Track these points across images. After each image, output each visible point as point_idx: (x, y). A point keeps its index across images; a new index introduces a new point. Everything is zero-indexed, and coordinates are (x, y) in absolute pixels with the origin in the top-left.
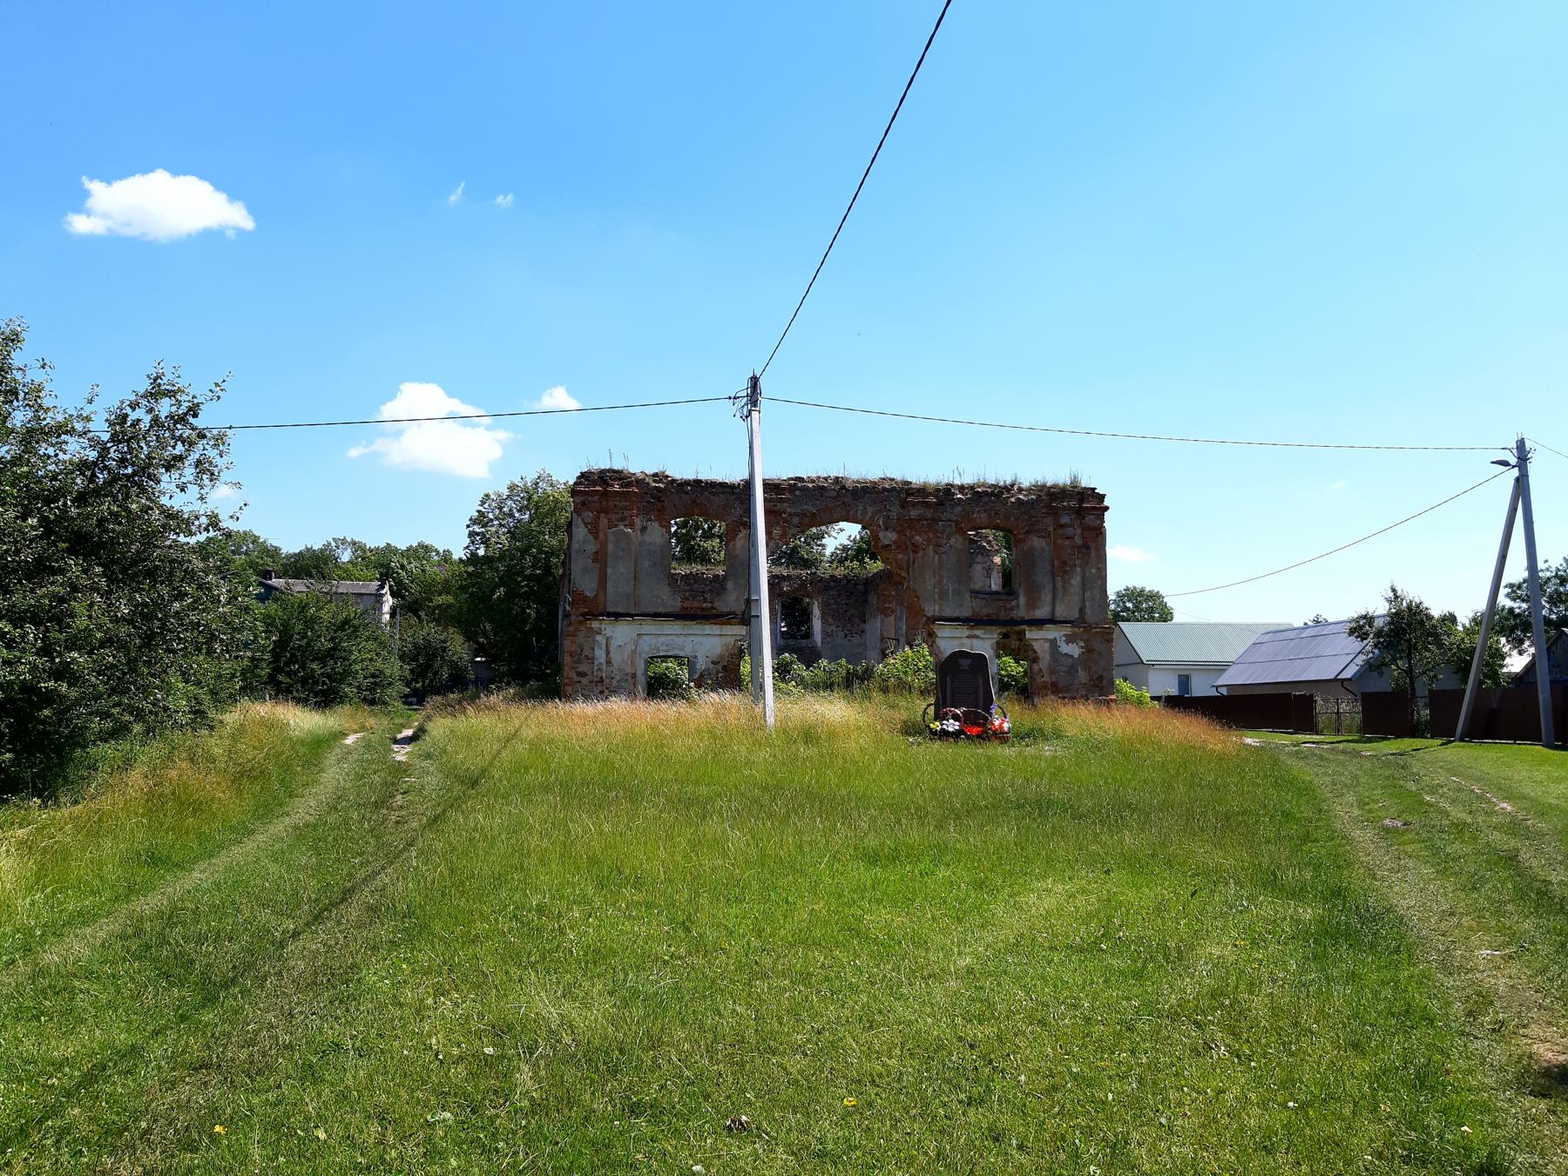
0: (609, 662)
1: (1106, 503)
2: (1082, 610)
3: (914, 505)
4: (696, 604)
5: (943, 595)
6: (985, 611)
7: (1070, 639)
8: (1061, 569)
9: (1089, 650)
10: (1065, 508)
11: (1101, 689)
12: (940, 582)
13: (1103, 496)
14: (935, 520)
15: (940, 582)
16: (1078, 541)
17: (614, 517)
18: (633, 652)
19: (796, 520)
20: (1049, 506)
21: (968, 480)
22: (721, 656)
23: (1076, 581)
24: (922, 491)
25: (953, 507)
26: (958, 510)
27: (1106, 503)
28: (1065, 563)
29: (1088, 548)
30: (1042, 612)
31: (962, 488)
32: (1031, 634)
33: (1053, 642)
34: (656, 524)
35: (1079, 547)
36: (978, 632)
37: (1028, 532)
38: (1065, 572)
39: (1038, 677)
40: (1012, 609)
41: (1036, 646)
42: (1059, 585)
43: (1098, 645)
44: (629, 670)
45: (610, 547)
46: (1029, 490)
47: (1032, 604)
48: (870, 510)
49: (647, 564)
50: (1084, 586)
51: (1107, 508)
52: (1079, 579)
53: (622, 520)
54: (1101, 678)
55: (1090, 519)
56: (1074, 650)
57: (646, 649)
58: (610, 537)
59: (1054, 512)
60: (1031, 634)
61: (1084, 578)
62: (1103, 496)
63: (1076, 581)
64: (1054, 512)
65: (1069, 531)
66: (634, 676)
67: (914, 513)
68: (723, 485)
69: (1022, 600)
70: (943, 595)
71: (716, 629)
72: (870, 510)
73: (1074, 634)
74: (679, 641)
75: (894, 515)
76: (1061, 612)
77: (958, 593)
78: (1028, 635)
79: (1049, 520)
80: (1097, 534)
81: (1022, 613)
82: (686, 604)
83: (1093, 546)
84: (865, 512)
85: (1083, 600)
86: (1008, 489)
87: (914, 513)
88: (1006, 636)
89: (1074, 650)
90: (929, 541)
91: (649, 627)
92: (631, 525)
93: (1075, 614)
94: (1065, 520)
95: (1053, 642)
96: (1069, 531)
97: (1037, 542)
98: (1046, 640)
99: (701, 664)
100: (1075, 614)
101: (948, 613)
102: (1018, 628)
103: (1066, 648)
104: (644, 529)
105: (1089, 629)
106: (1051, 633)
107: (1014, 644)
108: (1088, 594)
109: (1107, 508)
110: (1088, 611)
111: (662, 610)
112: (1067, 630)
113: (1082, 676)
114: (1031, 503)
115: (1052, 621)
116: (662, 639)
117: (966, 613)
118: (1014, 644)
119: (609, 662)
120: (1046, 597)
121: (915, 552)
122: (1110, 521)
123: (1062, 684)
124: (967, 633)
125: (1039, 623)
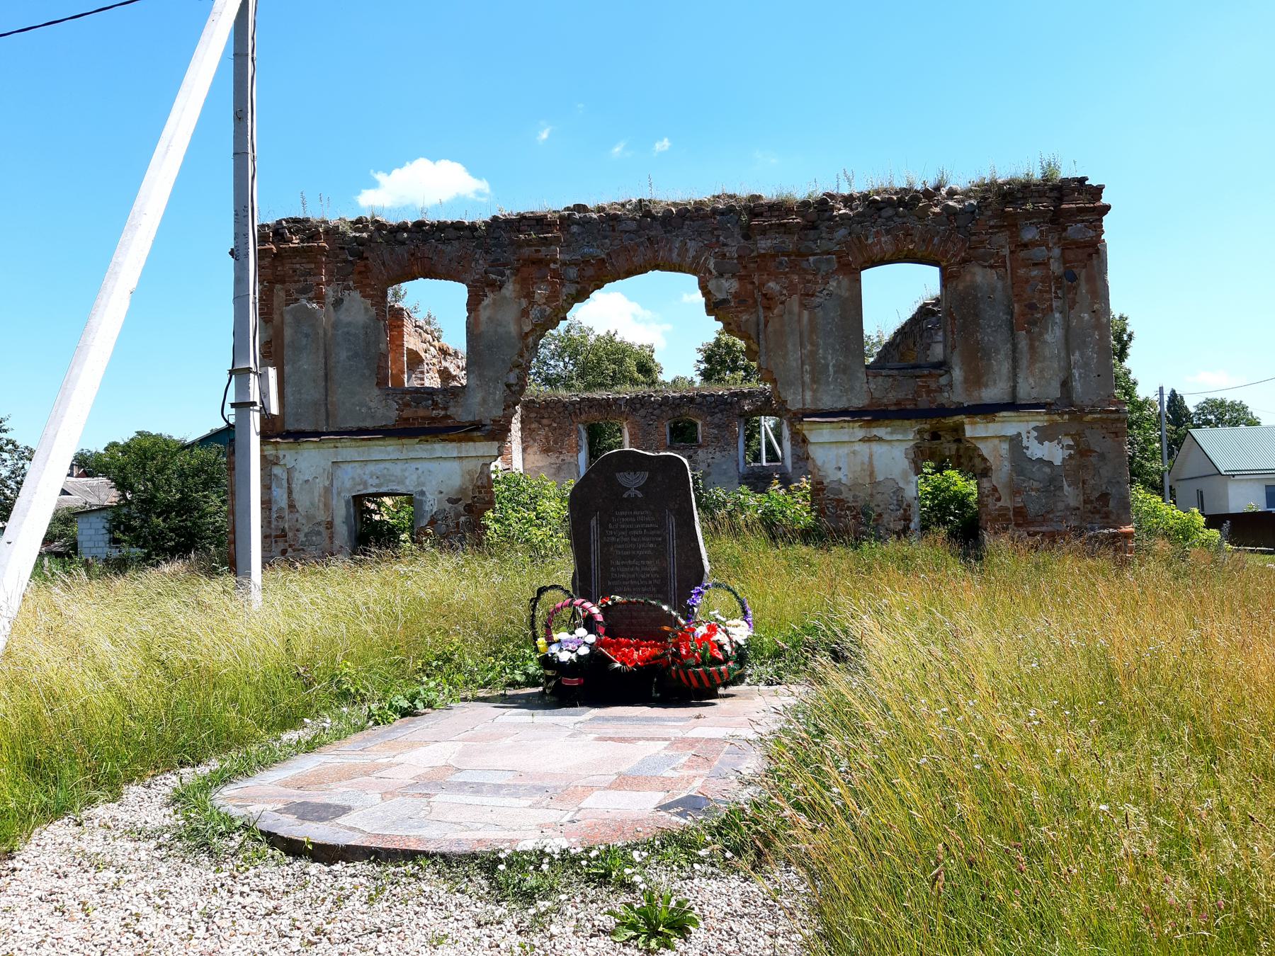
0: (292, 506)
1: (1105, 200)
2: (1066, 384)
3: (764, 231)
4: (421, 413)
5: (818, 375)
6: (892, 396)
7: (1044, 435)
8: (1026, 318)
9: (1081, 452)
10: (1029, 215)
11: (1107, 515)
12: (813, 354)
13: (1099, 189)
14: (802, 255)
15: (813, 354)
16: (1056, 267)
17: (292, 287)
18: (328, 490)
19: (573, 272)
20: (1003, 215)
21: (859, 187)
22: (462, 490)
23: (1053, 336)
24: (779, 208)
25: (831, 230)
26: (841, 233)
27: (1105, 200)
28: (1032, 307)
29: (1073, 278)
30: (994, 392)
31: (848, 200)
32: (974, 429)
33: (1015, 442)
34: (356, 295)
35: (1058, 279)
36: (880, 432)
37: (965, 261)
38: (1034, 323)
39: (990, 500)
40: (940, 390)
41: (985, 448)
42: (1023, 344)
43: (1096, 440)
44: (321, 516)
45: (288, 333)
46: (967, 194)
47: (976, 379)
48: (692, 246)
49: (344, 355)
50: (1068, 344)
51: (1107, 208)
52: (1058, 332)
53: (304, 291)
54: (1104, 497)
55: (1075, 230)
56: (1054, 452)
57: (348, 484)
58: (288, 318)
59: (1011, 224)
60: (974, 429)
61: (1067, 329)
62: (1099, 189)
64: (1011, 224)
65: (1039, 253)
66: (330, 525)
67: (764, 244)
68: (458, 226)
69: (957, 374)
70: (818, 375)
71: (452, 449)
72: (692, 246)
73: (1053, 425)
74: (397, 469)
75: (732, 251)
76: (1026, 390)
77: (842, 370)
78: (969, 432)
79: (1002, 238)
80: (1088, 256)
81: (959, 396)
82: (406, 414)
83: (1083, 274)
84: (684, 250)
85: (1068, 368)
86: (929, 194)
87: (764, 244)
88: (935, 436)
89: (1054, 452)
90: (792, 289)
91: (350, 450)
92: (319, 298)
93: (1054, 392)
94: (1029, 234)
95: (1015, 442)
96: (1039, 253)
97: (980, 276)
98: (1002, 438)
99: (432, 504)
100: (1054, 392)
101: (827, 402)
102: (950, 421)
103: (1037, 450)
104: (338, 303)
105: (1077, 413)
106: (1010, 425)
107: (949, 448)
108: (1076, 357)
109: (1107, 208)
110: (1077, 385)
111: (369, 424)
112: (1040, 419)
113: (1070, 495)
114: (970, 212)
115: (1013, 406)
116: (371, 468)
117: (859, 402)
119: (292, 506)
120: (1002, 366)
121: (768, 309)
122: (1115, 233)
123: (1033, 509)
124: (860, 433)
125: (987, 411)
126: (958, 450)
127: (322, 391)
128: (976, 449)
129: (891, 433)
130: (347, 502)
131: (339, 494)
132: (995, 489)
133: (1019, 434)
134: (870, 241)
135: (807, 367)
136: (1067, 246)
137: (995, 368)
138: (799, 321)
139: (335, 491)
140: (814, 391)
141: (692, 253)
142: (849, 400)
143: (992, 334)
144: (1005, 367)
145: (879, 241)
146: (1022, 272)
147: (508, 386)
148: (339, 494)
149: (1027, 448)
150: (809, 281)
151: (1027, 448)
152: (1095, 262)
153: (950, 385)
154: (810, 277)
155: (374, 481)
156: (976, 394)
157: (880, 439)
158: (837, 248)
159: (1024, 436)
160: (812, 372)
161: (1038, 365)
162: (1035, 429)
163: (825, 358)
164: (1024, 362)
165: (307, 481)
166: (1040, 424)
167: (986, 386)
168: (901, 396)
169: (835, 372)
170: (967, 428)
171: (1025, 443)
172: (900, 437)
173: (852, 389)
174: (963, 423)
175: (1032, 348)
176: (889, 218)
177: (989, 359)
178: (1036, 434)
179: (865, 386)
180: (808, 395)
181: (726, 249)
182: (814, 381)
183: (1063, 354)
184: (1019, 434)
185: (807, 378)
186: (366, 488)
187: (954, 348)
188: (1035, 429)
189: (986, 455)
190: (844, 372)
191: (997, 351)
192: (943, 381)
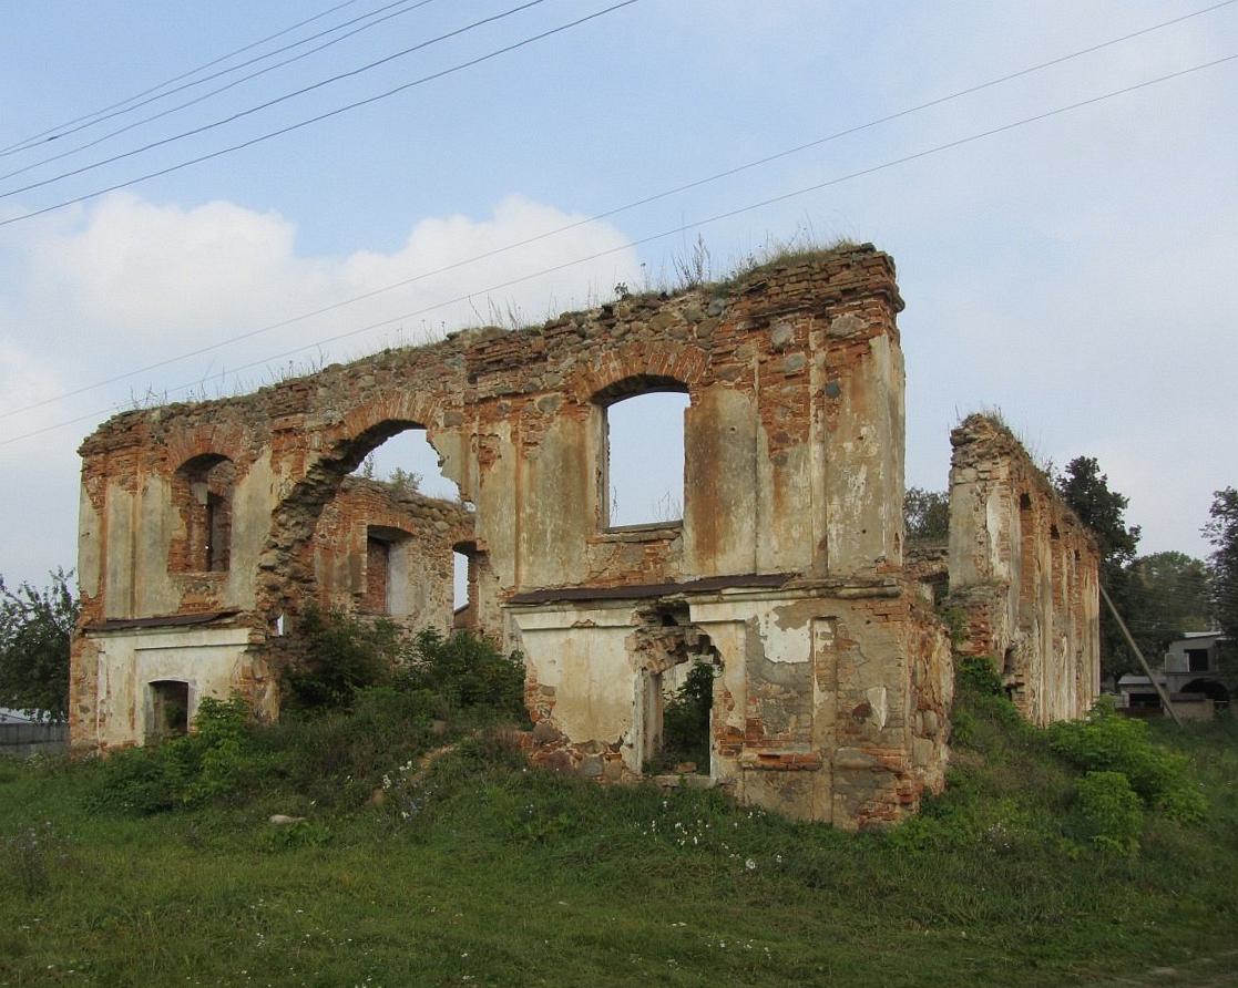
7: (787, 620)
9: (841, 643)
30: (730, 562)
50: (833, 482)
52: (816, 472)
57: (146, 671)
81: (686, 569)
110: (834, 548)
117: (575, 577)
120: (743, 524)
125: (712, 587)
127: (129, 579)
129: (606, 617)
130: (145, 689)
131: (140, 680)
132: (728, 694)
133: (756, 618)
137: (736, 526)
138: (517, 478)
139: (137, 678)
140: (531, 565)
142: (567, 575)
144: (747, 525)
145: (607, 369)
146: (770, 389)
148: (140, 680)
149: (765, 637)
150: (532, 427)
151: (765, 637)
152: (864, 366)
154: (534, 422)
156: (710, 562)
157: (595, 627)
159: (762, 620)
161: (783, 521)
162: (776, 610)
163: (543, 523)
164: (767, 518)
165: (118, 668)
167: (724, 552)
169: (553, 540)
170: (693, 610)
171: (762, 630)
177: (728, 515)
178: (777, 618)
181: (452, 396)
184: (756, 618)
188: (776, 610)
190: (562, 539)
191: (738, 503)
192: (675, 545)
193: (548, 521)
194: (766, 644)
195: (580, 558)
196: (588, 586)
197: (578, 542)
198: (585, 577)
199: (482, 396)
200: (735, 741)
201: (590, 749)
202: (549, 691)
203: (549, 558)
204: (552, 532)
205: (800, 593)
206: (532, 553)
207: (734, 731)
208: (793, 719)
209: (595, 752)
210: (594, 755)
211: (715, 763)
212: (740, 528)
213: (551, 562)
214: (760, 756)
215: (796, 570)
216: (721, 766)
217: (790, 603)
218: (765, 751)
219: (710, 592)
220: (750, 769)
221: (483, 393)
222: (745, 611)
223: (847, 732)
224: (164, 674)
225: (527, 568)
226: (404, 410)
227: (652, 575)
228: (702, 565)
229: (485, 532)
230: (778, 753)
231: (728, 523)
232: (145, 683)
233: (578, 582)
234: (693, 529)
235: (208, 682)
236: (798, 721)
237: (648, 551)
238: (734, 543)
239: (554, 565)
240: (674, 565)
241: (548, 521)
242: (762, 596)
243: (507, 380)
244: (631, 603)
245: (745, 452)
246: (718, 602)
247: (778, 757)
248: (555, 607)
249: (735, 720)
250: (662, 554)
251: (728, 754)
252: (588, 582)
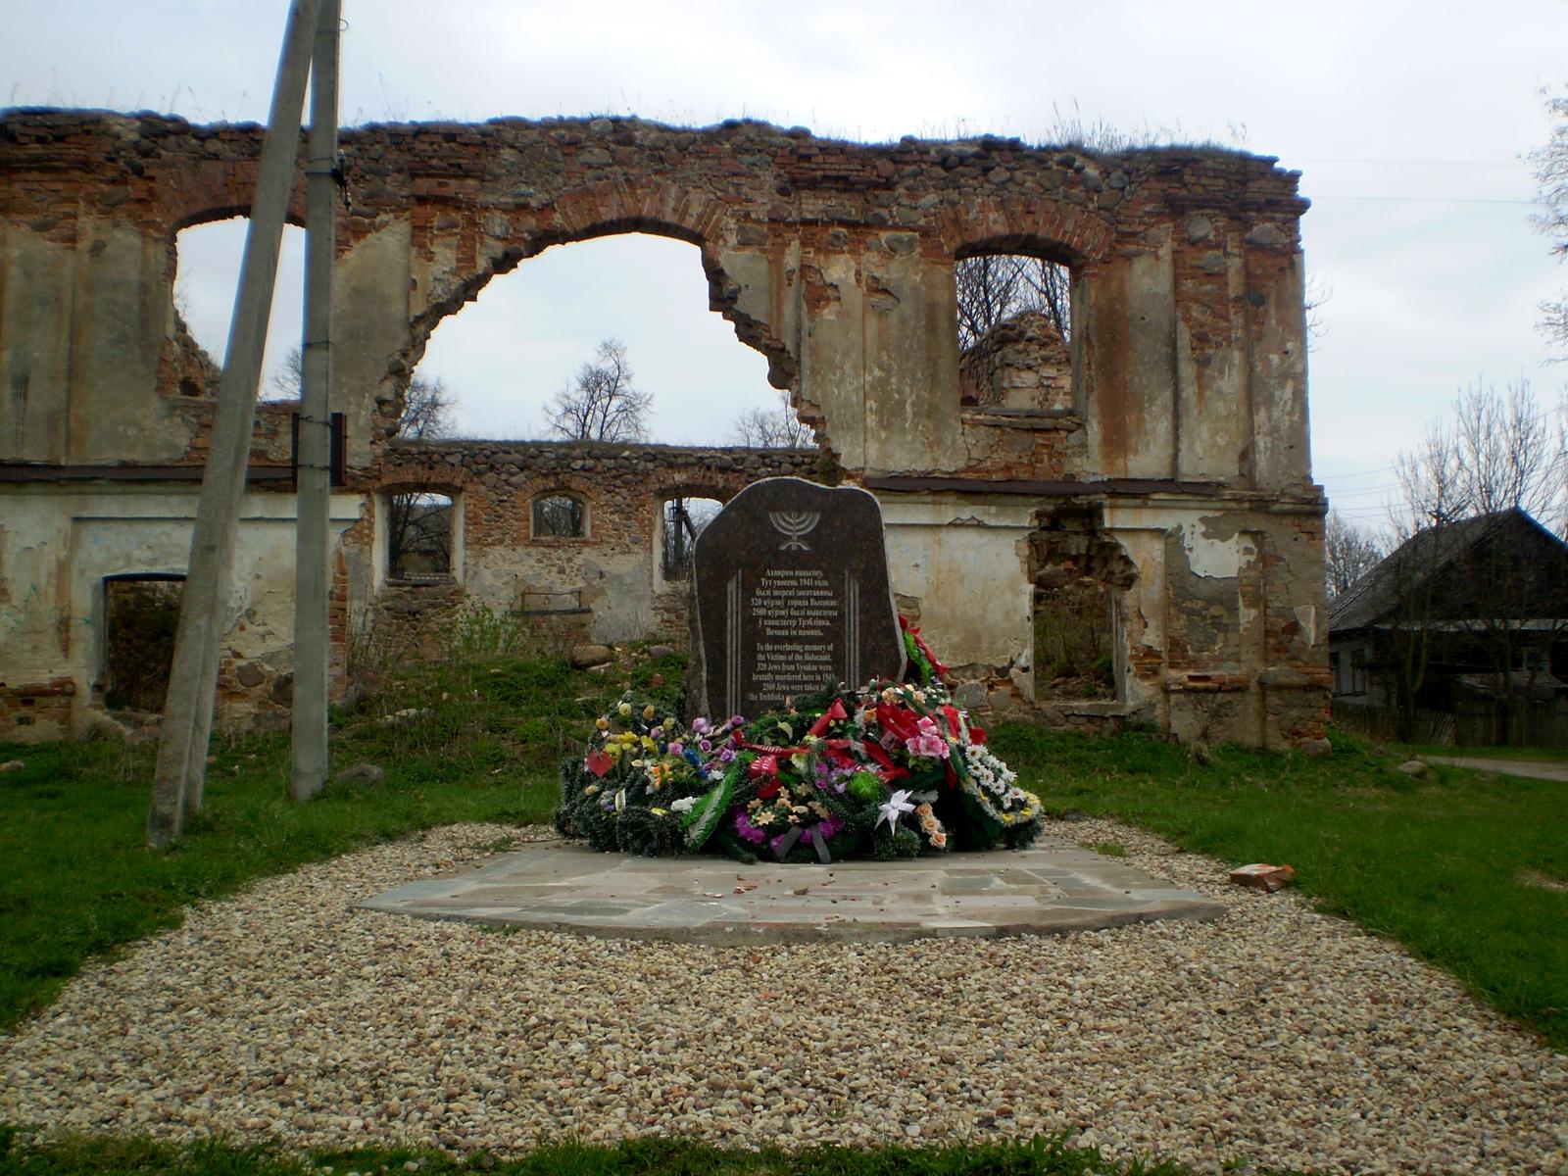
2: (1246, 455)
7: (1215, 531)
9: (1267, 560)
13: (1294, 177)
18: (63, 568)
27: (1303, 192)
30: (1146, 462)
32: (1116, 518)
33: (1171, 539)
42: (1189, 391)
47: (1117, 442)
50: (1253, 395)
60: (1116, 518)
62: (1294, 177)
63: (1230, 382)
66: (64, 625)
69: (1094, 430)
80: (1274, 273)
85: (1251, 430)
107: (1078, 544)
108: (1261, 417)
110: (1262, 461)
117: (948, 463)
118: (1078, 544)
125: (1135, 491)
126: (1089, 548)
128: (1117, 547)
129: (997, 515)
131: (82, 573)
133: (1180, 528)
134: (972, 215)
135: (872, 404)
136: (1252, 247)
137: (1149, 426)
140: (883, 443)
141: (696, 209)
142: (935, 460)
143: (1143, 373)
144: (1163, 426)
145: (986, 219)
147: (381, 402)
151: (1191, 550)
152: (1289, 281)
153: (1084, 445)
155: (146, 554)
156: (1120, 462)
158: (922, 222)
159: (1186, 530)
160: (879, 412)
163: (900, 392)
166: (1210, 514)
167: (1136, 452)
168: (1013, 458)
169: (915, 415)
170: (1106, 512)
172: (1009, 523)
173: (939, 442)
174: (1100, 507)
175: (1201, 396)
176: (1001, 186)
177: (1141, 411)
178: (1203, 529)
179: (960, 440)
180: (873, 448)
181: (750, 207)
182: (884, 425)
183: (1242, 412)
185: (872, 421)
186: (129, 563)
187: (1090, 389)
188: (1203, 520)
189: (1132, 558)
190: (930, 414)
191: (1152, 400)
192: (1075, 438)
193: (907, 390)
194: (1192, 557)
195: (954, 441)
196: (963, 475)
197: (953, 421)
198: (962, 464)
199: (809, 216)
200: (1149, 663)
201: (969, 674)
202: (911, 602)
203: (909, 438)
204: (913, 404)
205: (1233, 505)
206: (884, 428)
207: (1150, 652)
208: (1221, 637)
209: (975, 677)
210: (973, 682)
211: (1131, 688)
212: (1154, 429)
213: (913, 441)
214: (1191, 678)
215: (1222, 479)
216: (1137, 692)
217: (1218, 514)
218: (1192, 673)
219: (1134, 496)
220: (1178, 692)
221: (811, 212)
222: (1166, 521)
223: (1277, 651)
224: (154, 561)
225: (877, 445)
226: (669, 210)
227: (1045, 468)
228: (1111, 464)
229: (819, 394)
230: (1209, 674)
231: (1140, 421)
232: (97, 577)
233: (952, 470)
234: (1100, 423)
235: (258, 577)
236: (1226, 640)
237: (1040, 441)
238: (1148, 444)
239: (918, 446)
240: (1077, 461)
241: (907, 390)
242: (1191, 504)
243: (847, 203)
244: (1034, 500)
245: (1159, 345)
246: (1140, 507)
247: (1207, 678)
248: (930, 499)
249: (1152, 638)
250: (1058, 446)
251: (1144, 677)
252: (964, 471)
